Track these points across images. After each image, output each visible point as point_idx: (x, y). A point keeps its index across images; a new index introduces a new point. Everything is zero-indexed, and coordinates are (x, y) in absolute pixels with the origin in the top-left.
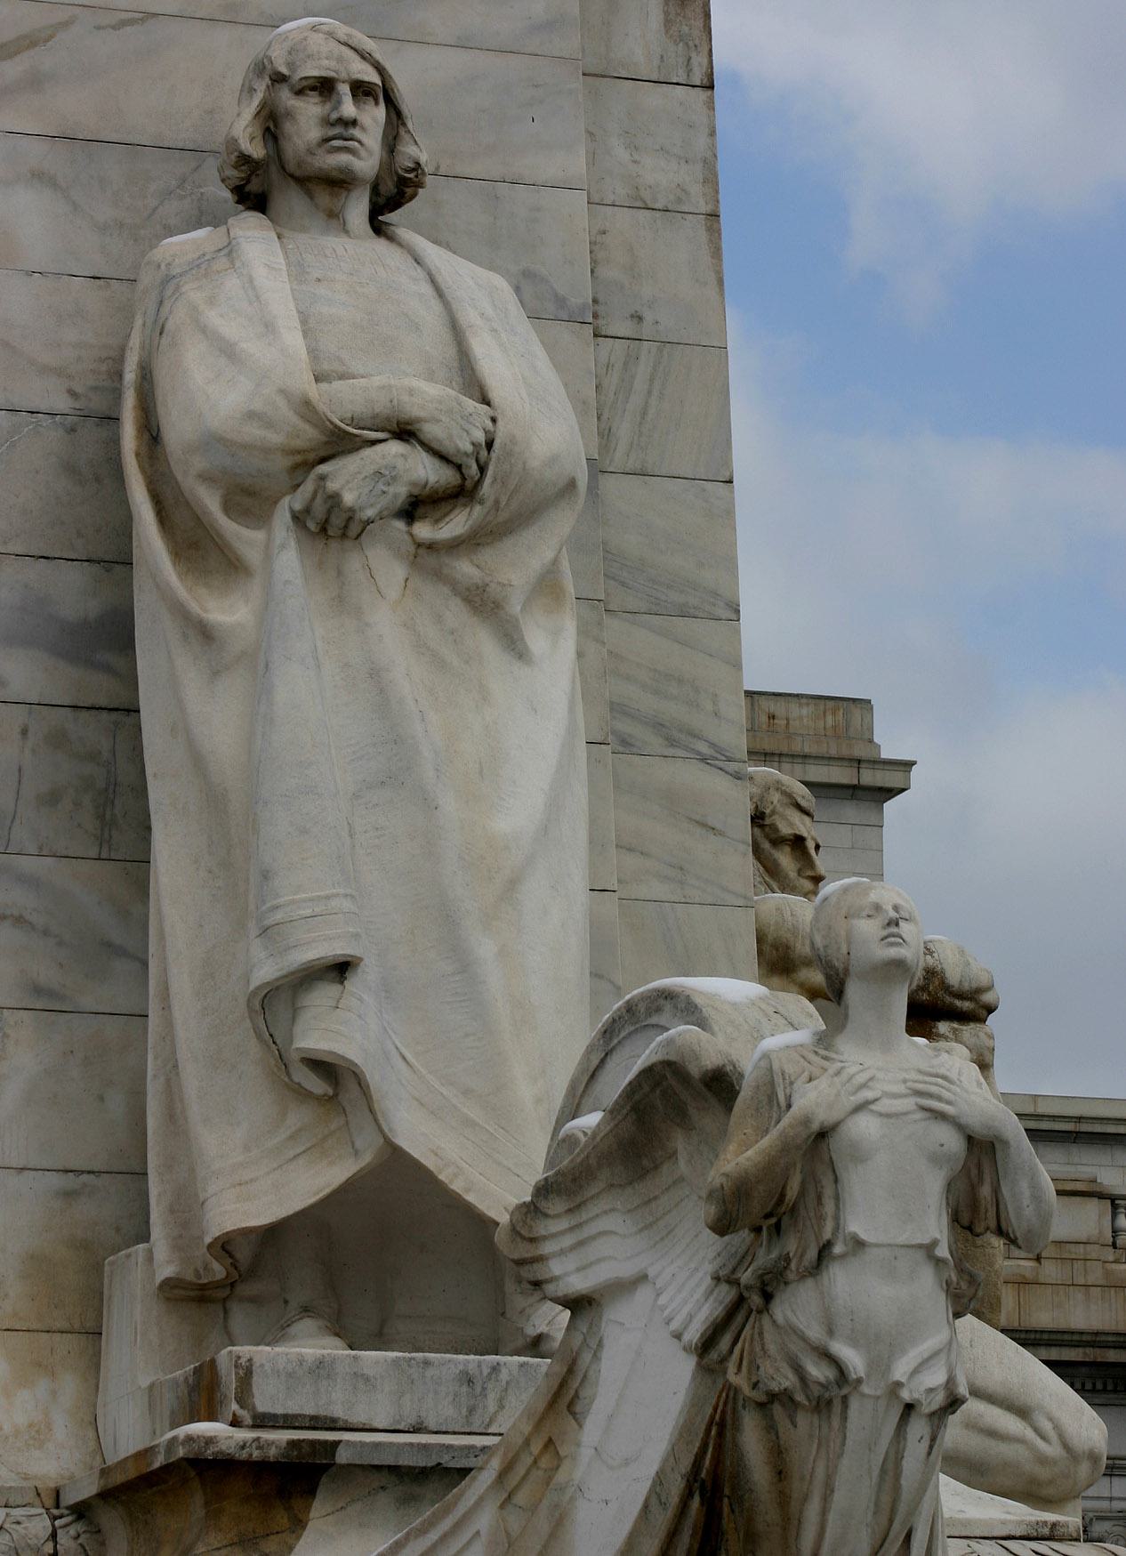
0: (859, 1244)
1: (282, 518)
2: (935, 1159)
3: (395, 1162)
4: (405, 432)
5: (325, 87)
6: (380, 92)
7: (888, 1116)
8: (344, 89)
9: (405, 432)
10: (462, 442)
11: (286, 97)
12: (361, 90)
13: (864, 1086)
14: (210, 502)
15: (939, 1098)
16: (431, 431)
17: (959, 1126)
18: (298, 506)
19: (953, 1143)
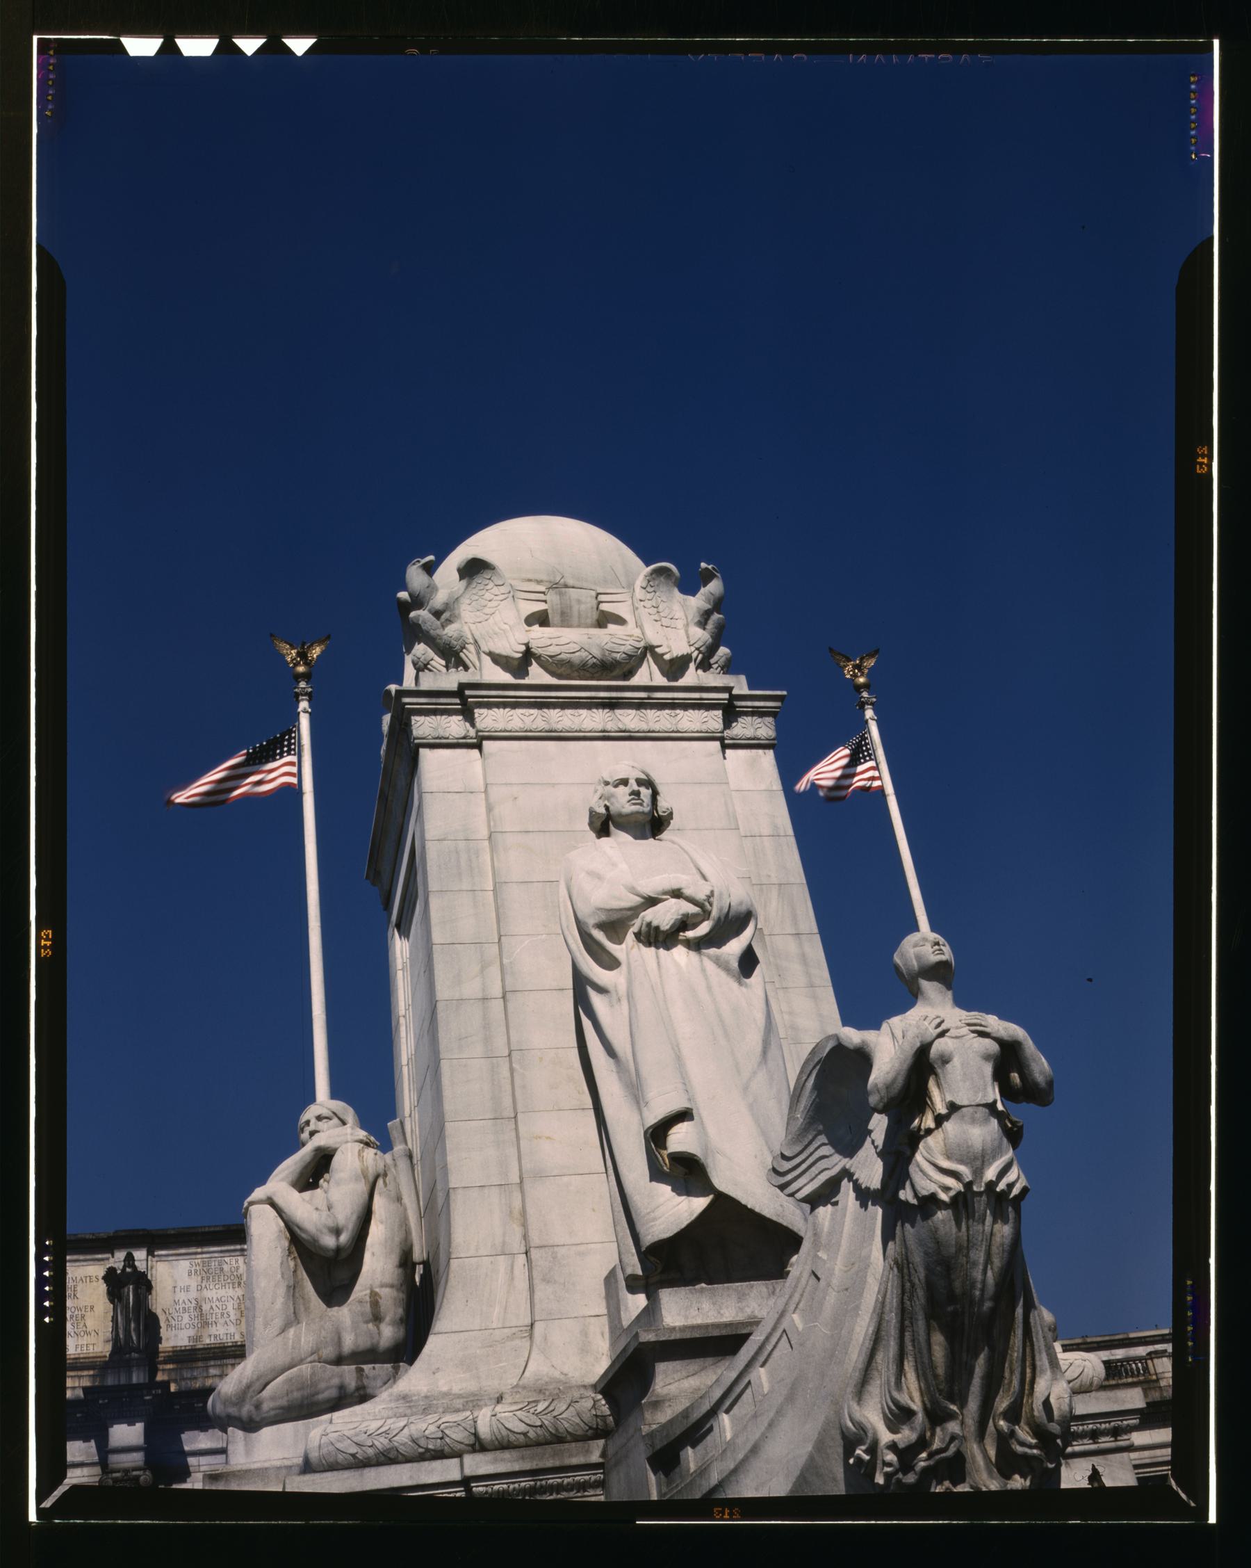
0: (953, 1108)
1: (630, 937)
2: (987, 1057)
3: (725, 1205)
4: (677, 894)
5: (624, 782)
6: (648, 783)
7: (957, 1037)
8: (632, 783)
9: (677, 894)
10: (701, 896)
11: (610, 788)
12: (640, 782)
13: (939, 1025)
14: (599, 935)
15: (981, 1025)
16: (687, 892)
17: (996, 1039)
18: (636, 931)
19: (994, 1047)
